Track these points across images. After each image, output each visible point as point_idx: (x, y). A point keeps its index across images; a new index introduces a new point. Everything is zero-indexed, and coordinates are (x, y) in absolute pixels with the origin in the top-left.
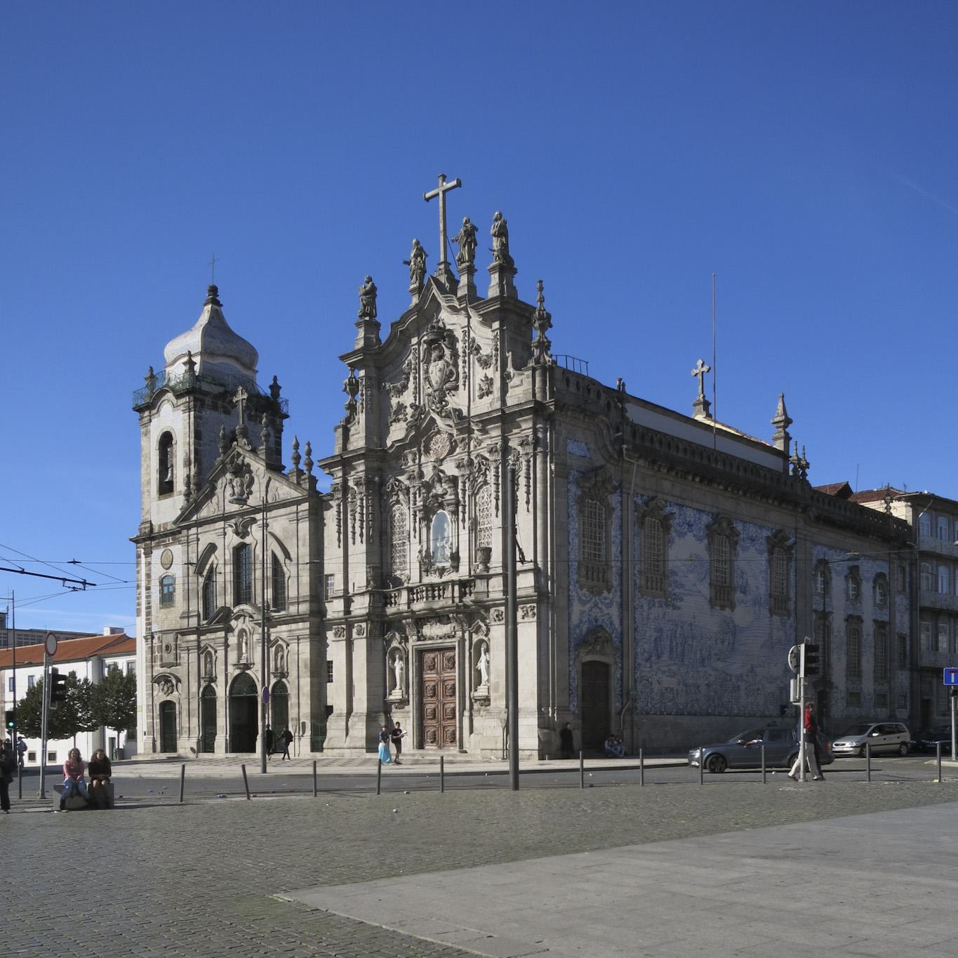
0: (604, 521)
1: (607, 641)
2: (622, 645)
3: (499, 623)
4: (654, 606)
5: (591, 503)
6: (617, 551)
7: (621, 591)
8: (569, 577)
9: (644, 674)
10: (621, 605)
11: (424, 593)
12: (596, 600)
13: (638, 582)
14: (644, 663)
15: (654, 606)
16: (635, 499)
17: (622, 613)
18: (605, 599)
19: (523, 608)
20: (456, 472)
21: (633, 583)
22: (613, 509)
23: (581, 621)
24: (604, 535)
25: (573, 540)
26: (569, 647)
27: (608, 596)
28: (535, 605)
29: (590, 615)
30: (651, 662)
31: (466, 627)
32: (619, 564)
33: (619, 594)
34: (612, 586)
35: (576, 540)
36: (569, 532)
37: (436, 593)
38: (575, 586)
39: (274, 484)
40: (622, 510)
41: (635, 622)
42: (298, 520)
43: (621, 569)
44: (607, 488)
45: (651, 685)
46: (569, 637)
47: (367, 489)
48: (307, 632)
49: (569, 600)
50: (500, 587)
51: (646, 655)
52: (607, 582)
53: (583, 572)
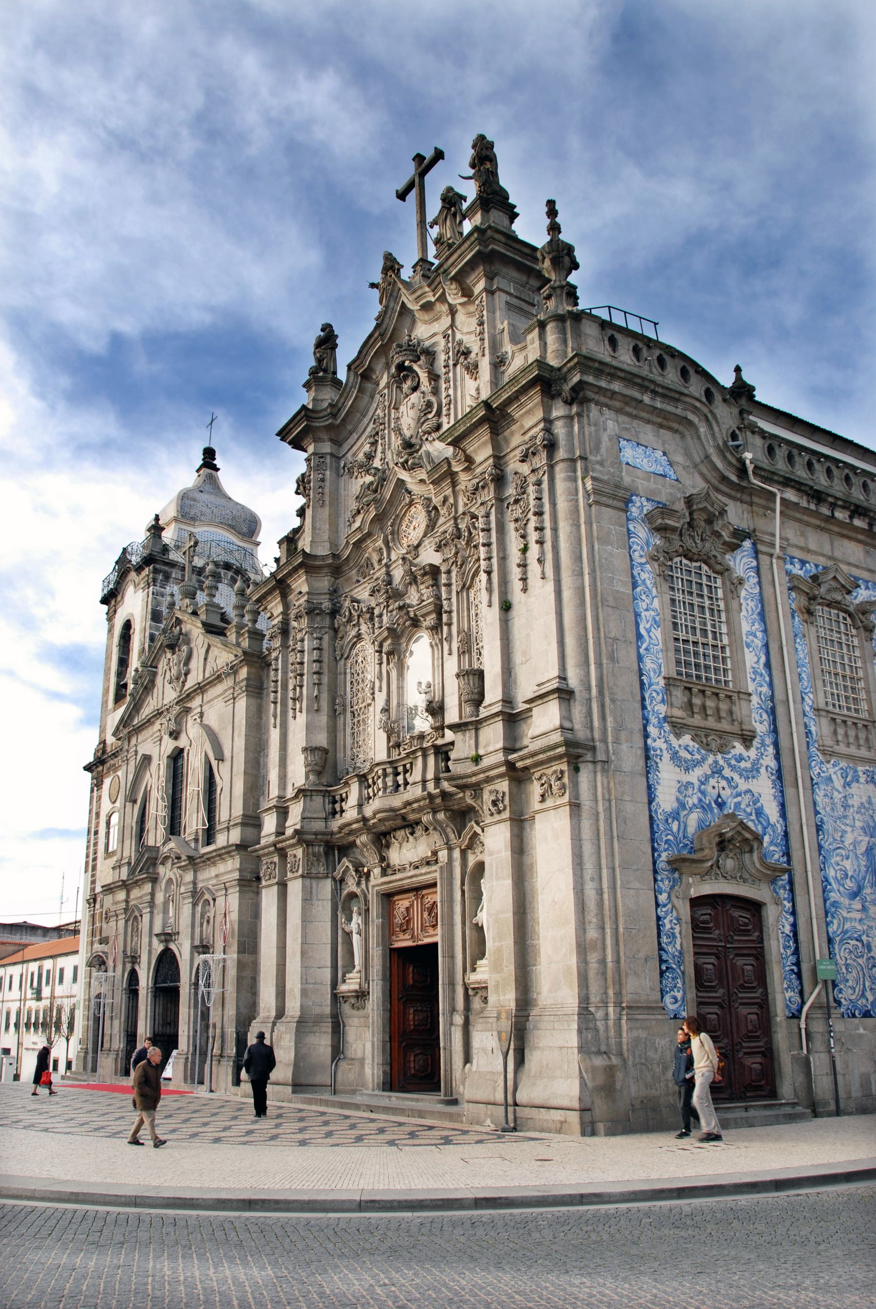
0: (722, 604)
1: (751, 851)
2: (789, 862)
3: (497, 817)
4: (858, 781)
5: (686, 565)
6: (758, 662)
7: (776, 745)
8: (644, 707)
9: (847, 926)
10: (779, 775)
11: (380, 781)
12: (716, 762)
13: (813, 729)
14: (846, 901)
15: (858, 781)
16: (789, 567)
17: (782, 792)
18: (740, 759)
19: (540, 778)
20: (436, 559)
21: (802, 728)
22: (741, 582)
23: (682, 805)
24: (724, 629)
25: (648, 631)
26: (654, 863)
27: (745, 753)
28: (564, 767)
29: (703, 793)
30: (864, 901)
31: (454, 840)
32: (765, 689)
33: (771, 750)
34: (754, 732)
35: (657, 633)
36: (637, 615)
37: (400, 779)
38: (661, 727)
39: (214, 652)
40: (759, 583)
41: (817, 813)
42: (234, 699)
43: (772, 698)
44: (719, 536)
45: (869, 949)
46: (653, 840)
47: (311, 621)
48: (236, 875)
49: (647, 758)
50: (497, 742)
51: (849, 884)
52: (741, 723)
53: (679, 695)
